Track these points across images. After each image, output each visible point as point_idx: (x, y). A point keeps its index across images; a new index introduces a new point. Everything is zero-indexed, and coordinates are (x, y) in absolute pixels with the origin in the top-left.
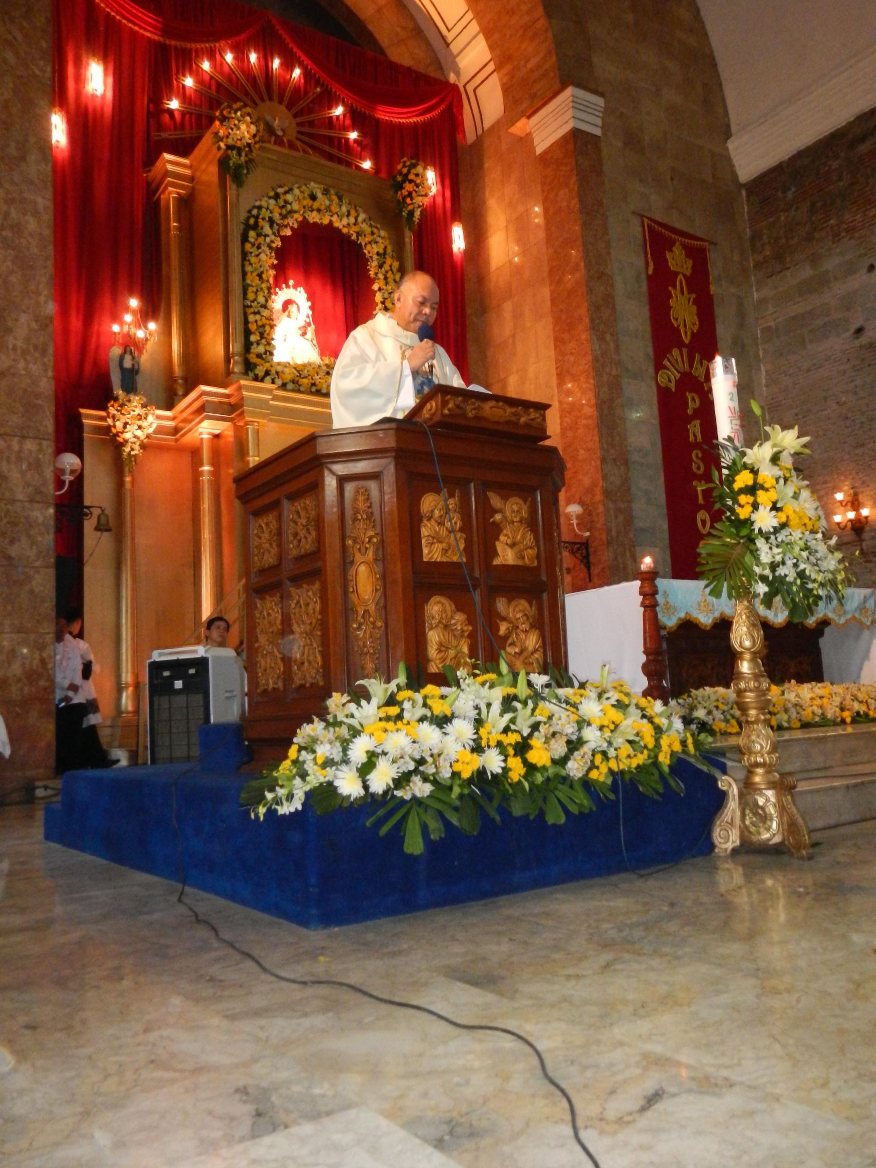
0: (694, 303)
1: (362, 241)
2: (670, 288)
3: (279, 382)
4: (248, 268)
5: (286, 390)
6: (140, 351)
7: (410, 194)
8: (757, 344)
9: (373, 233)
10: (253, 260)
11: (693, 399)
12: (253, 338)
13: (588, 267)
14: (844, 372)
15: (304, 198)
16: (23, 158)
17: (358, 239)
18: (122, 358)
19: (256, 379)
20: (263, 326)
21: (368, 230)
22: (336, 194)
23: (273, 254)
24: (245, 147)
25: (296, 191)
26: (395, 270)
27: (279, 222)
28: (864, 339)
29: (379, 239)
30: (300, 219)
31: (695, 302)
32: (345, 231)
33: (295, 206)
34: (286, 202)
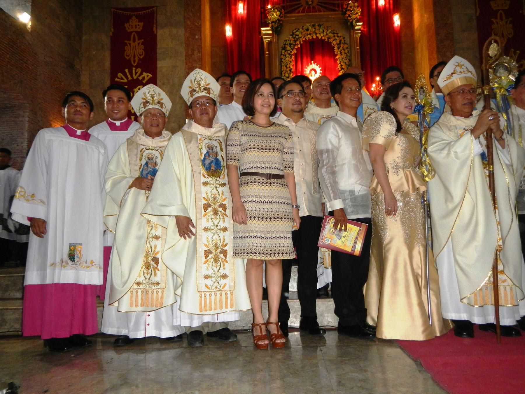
1: (330, 41)
4: (283, 64)
7: (349, 15)
10: (284, 61)
16: (193, 54)
17: (328, 40)
21: (332, 35)
22: (318, 26)
23: (293, 57)
24: (276, 21)
25: (301, 30)
26: (345, 48)
29: (337, 38)
30: (304, 39)
32: (323, 38)
33: (300, 36)
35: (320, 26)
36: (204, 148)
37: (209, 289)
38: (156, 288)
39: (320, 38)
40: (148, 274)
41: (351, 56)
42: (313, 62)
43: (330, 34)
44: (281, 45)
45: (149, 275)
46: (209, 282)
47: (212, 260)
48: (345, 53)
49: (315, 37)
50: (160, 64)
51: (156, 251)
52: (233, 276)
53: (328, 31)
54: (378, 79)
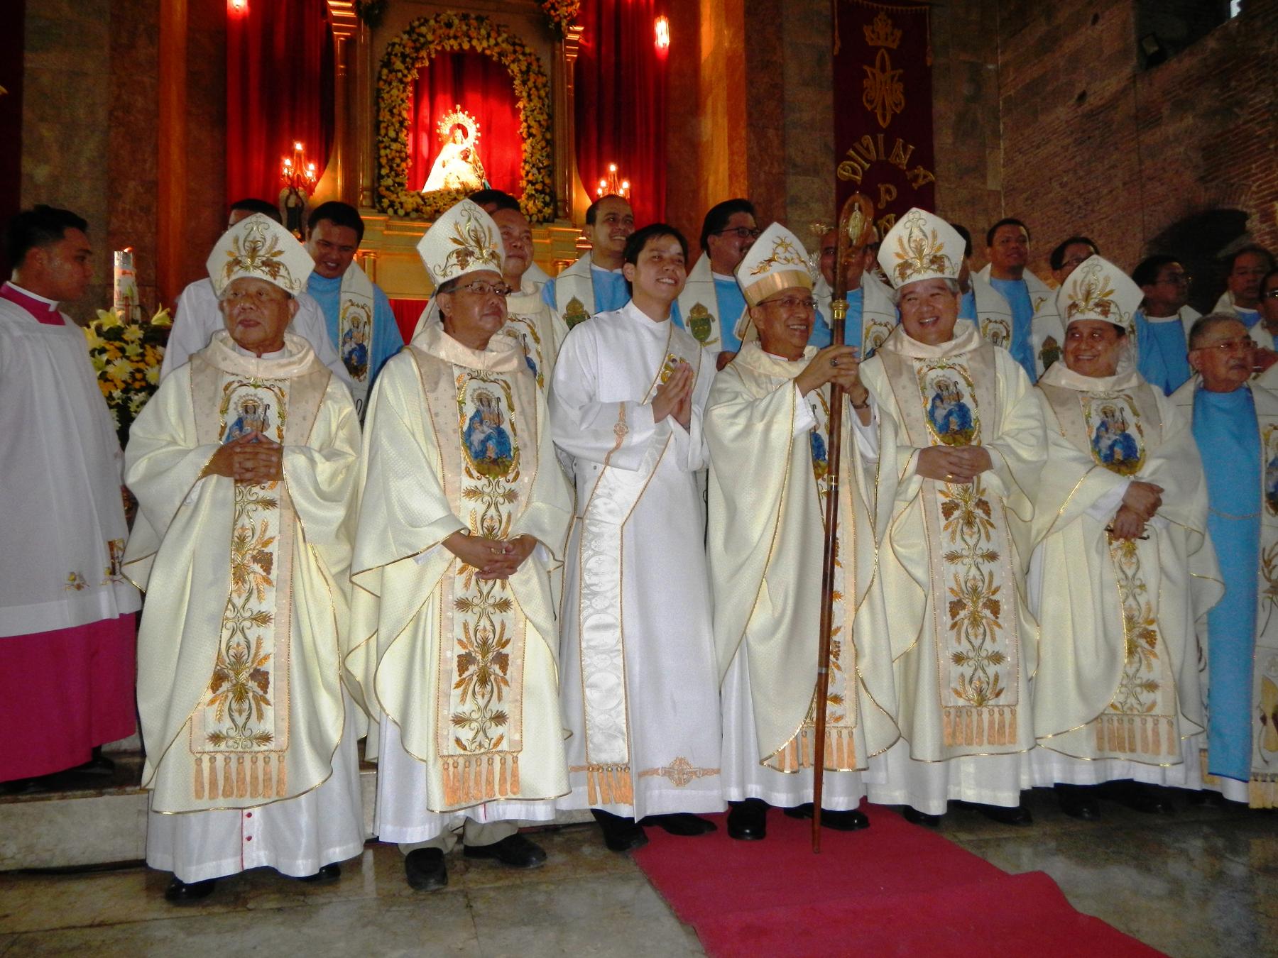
0: (899, 80)
1: (505, 61)
2: (865, 67)
3: (401, 212)
4: (382, 105)
5: (412, 220)
6: (310, 189)
7: (553, 5)
8: (998, 119)
9: (515, 52)
10: (386, 96)
11: (888, 191)
12: (384, 172)
13: (749, 58)
14: (1065, 148)
15: (440, 28)
18: (288, 198)
19: (383, 211)
20: (393, 159)
21: (511, 48)
23: (410, 89)
25: (432, 22)
27: (414, 55)
28: (1086, 107)
29: (521, 57)
30: (439, 48)
31: (899, 80)
32: (488, 52)
33: (430, 37)
34: (421, 35)
35: (480, 19)
36: (468, 401)
37: (465, 749)
38: (263, 748)
39: (479, 50)
40: (240, 712)
41: (552, 107)
42: (458, 107)
43: (504, 45)
44: (380, 51)
45: (245, 715)
46: (466, 734)
47: (475, 678)
48: (540, 97)
49: (466, 46)
50: (32, 61)
51: (262, 654)
52: (518, 717)
53: (499, 35)
54: (613, 168)
